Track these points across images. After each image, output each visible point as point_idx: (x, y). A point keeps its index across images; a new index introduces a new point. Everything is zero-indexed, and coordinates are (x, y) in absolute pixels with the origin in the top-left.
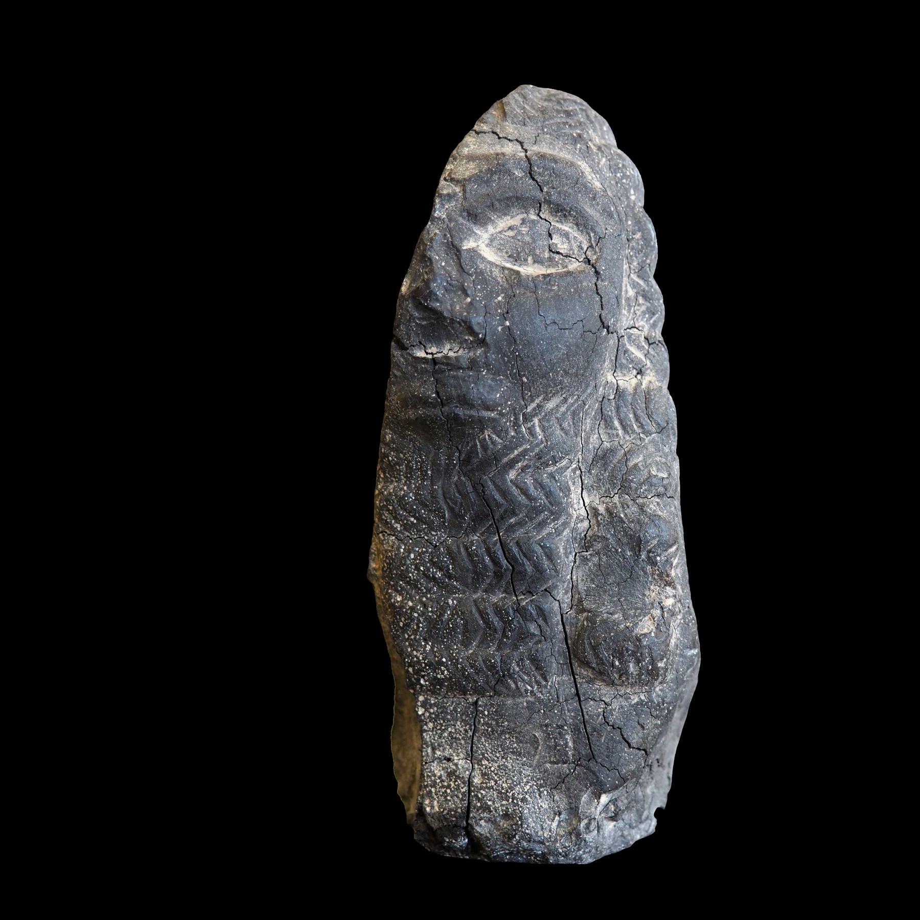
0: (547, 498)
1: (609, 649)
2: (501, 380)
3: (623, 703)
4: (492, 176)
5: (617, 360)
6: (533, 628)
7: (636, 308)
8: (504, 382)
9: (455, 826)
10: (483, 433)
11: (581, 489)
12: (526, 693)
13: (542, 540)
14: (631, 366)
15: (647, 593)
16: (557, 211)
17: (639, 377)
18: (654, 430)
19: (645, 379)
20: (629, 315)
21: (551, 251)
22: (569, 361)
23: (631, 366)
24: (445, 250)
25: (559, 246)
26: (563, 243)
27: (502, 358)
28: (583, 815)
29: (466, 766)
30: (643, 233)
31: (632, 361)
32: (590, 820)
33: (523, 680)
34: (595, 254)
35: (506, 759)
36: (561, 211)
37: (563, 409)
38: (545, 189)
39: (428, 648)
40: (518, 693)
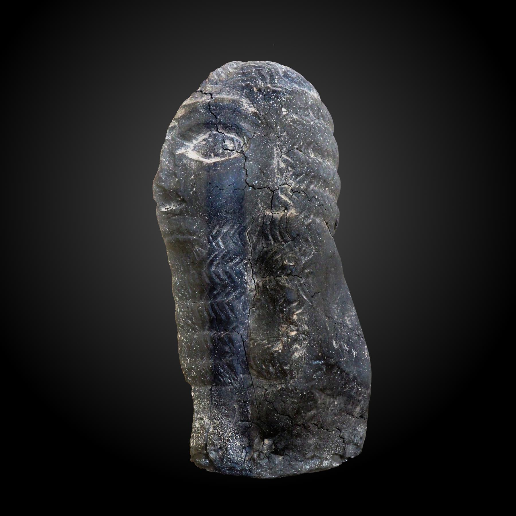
0: (229, 279)
1: (259, 359)
2: (195, 219)
3: (274, 390)
4: (190, 114)
5: (272, 203)
6: (227, 348)
7: (287, 173)
8: (197, 220)
9: (200, 453)
10: (194, 248)
11: (252, 274)
12: (229, 384)
13: (228, 302)
14: (280, 205)
15: (280, 329)
16: (226, 128)
17: (286, 211)
18: (289, 239)
19: (289, 212)
20: (282, 178)
21: (223, 149)
22: (227, 206)
23: (280, 205)
24: (169, 156)
25: (228, 146)
26: (230, 144)
27: (194, 207)
28: (256, 450)
29: (208, 422)
30: (287, 131)
31: (281, 203)
32: (259, 453)
33: (226, 377)
34: (246, 148)
35: (223, 419)
36: (227, 127)
37: (232, 232)
38: (218, 117)
39: (189, 361)
40: (225, 384)
